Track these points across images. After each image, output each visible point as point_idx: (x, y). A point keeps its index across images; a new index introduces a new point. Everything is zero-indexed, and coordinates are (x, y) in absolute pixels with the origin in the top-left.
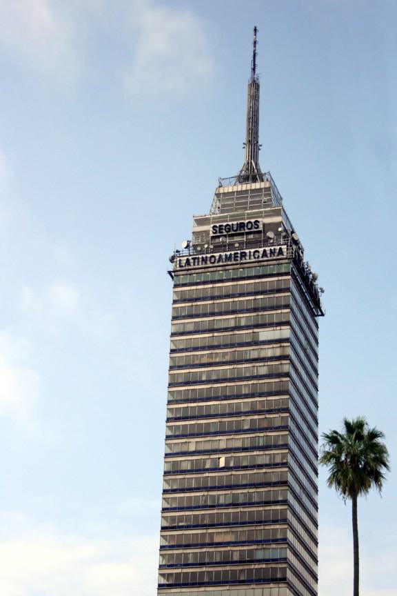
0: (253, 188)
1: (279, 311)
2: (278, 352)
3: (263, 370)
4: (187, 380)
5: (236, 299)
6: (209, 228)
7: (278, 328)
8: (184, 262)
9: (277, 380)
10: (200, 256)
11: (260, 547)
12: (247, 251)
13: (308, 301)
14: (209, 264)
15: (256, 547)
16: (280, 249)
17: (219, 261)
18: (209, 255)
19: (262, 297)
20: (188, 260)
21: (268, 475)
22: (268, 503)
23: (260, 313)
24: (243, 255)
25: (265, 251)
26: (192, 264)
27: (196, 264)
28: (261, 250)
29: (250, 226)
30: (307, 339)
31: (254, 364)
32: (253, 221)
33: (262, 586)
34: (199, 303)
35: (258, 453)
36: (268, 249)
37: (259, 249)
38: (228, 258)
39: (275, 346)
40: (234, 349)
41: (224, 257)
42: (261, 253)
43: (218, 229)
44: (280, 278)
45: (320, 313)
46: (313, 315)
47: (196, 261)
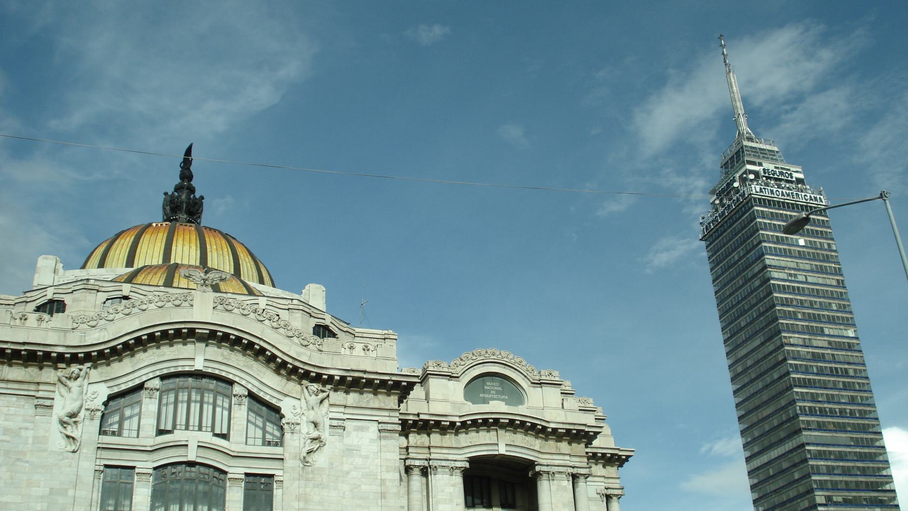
2: (760, 266)
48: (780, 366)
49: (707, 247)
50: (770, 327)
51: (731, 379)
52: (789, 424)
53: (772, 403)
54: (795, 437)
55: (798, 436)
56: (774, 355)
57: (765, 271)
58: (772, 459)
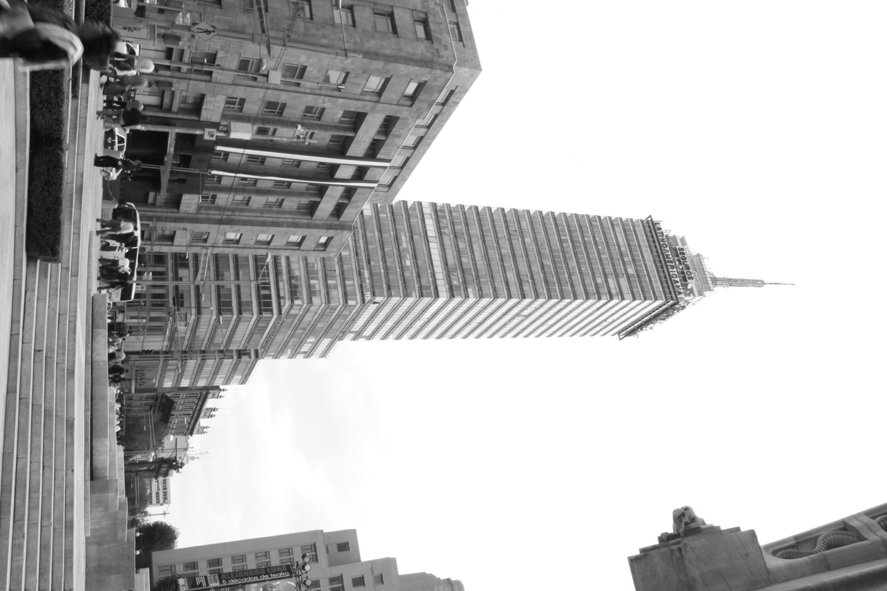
1: (641, 293)
2: (613, 291)
3: (599, 280)
4: (582, 227)
5: (642, 262)
6: (680, 246)
7: (630, 292)
9: (595, 292)
11: (474, 278)
13: (650, 314)
15: (474, 274)
19: (648, 280)
21: (527, 284)
22: (507, 284)
23: (637, 279)
28: (678, 279)
29: (689, 273)
30: (614, 321)
31: (602, 274)
33: (445, 278)
34: (634, 236)
35: (542, 276)
36: (679, 284)
39: (617, 289)
40: (609, 260)
43: (682, 251)
44: (662, 293)
45: (621, 337)
46: (619, 333)
48: (518, 287)
49: (642, 221)
50: (556, 284)
51: (516, 210)
52: (461, 281)
53: (485, 263)
54: (447, 286)
55: (448, 290)
56: (530, 281)
57: (608, 295)
58: (435, 268)
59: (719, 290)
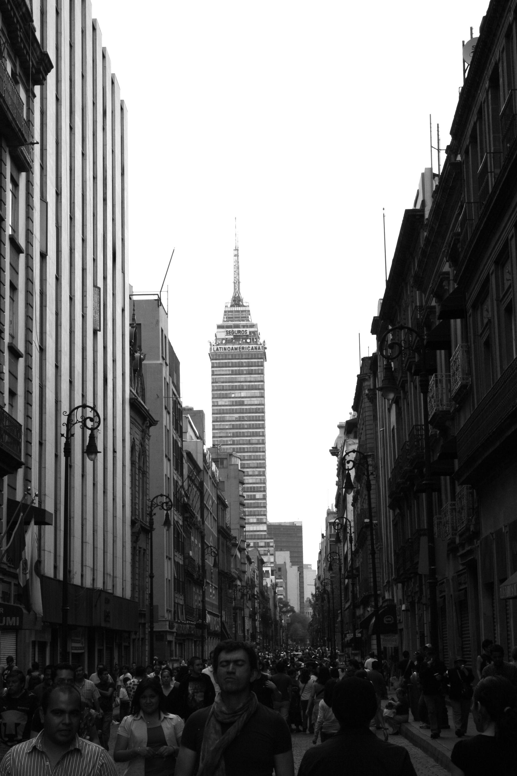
0: (242, 310)
8: (215, 349)
10: (223, 347)
12: (245, 346)
14: (227, 351)
16: (259, 347)
17: (232, 350)
18: (227, 346)
20: (217, 348)
24: (243, 348)
25: (252, 347)
26: (219, 350)
27: (221, 350)
32: (244, 329)
36: (254, 346)
37: (250, 346)
38: (236, 349)
41: (234, 348)
42: (251, 348)
47: (221, 349)
59: (244, 295)
